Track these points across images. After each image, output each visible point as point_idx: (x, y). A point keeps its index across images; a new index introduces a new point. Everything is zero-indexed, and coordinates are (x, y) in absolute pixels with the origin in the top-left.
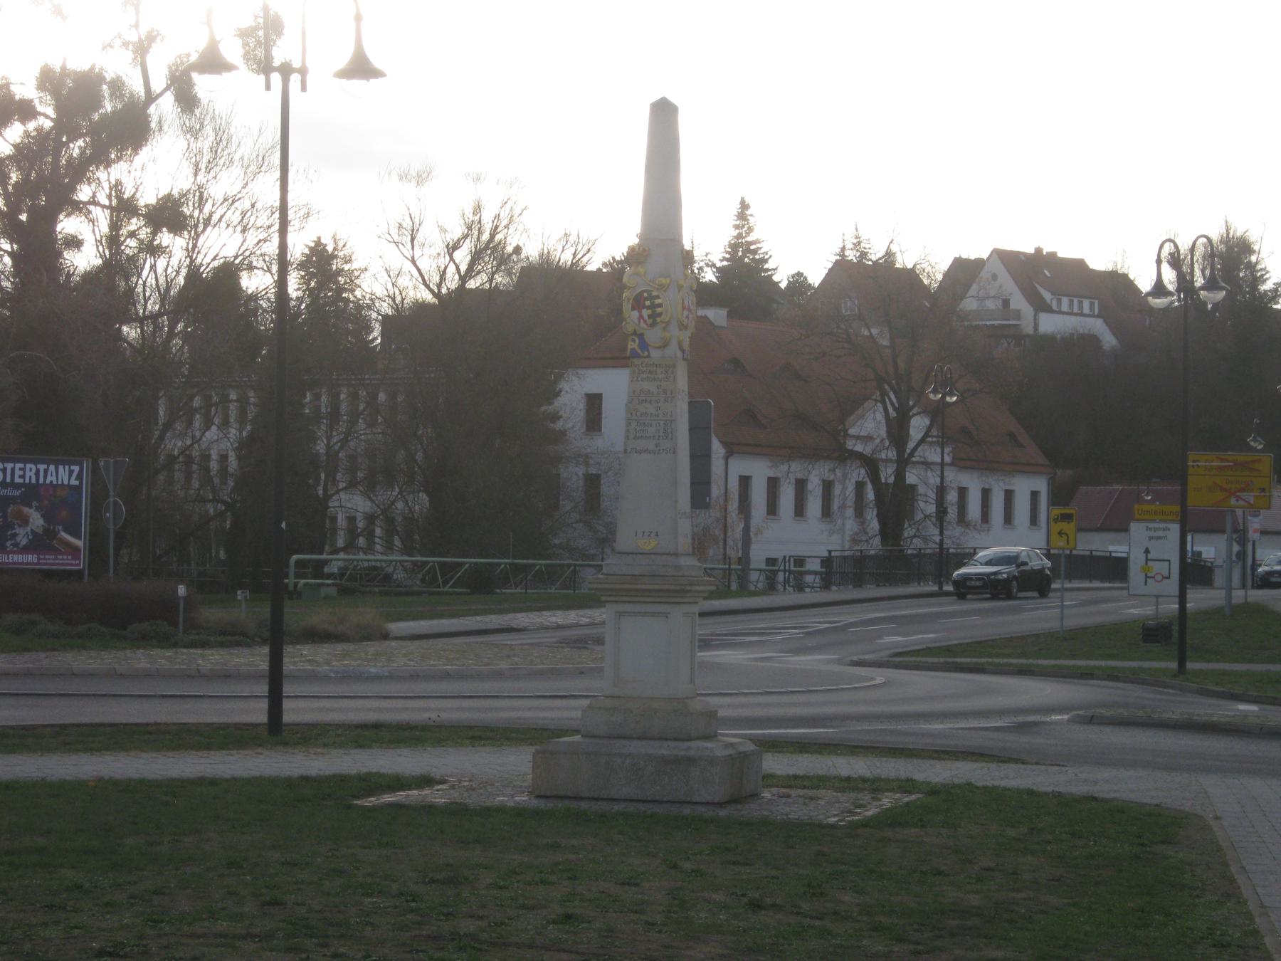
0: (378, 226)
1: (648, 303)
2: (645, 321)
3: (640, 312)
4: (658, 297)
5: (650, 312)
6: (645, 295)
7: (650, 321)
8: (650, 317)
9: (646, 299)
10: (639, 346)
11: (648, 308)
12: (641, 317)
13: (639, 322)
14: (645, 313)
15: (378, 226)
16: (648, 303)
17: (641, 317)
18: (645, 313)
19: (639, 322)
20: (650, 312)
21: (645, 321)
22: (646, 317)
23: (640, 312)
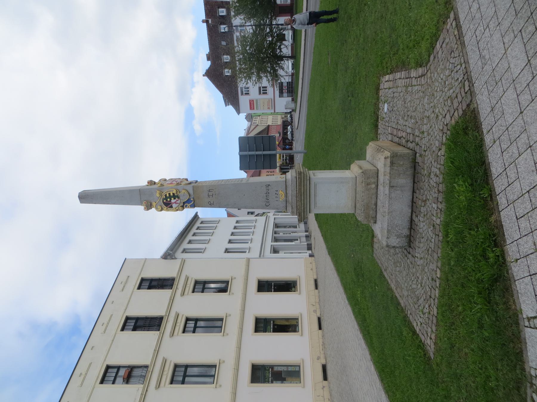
1: (169, 200)
3: (173, 203)
5: (172, 199)
6: (165, 201)
9: (167, 200)
10: (189, 204)
11: (171, 200)
12: (175, 203)
13: (177, 203)
16: (169, 200)
17: (175, 203)
18: (173, 201)
19: (177, 203)
20: (172, 199)
21: (177, 201)
22: (175, 200)
23: (173, 203)
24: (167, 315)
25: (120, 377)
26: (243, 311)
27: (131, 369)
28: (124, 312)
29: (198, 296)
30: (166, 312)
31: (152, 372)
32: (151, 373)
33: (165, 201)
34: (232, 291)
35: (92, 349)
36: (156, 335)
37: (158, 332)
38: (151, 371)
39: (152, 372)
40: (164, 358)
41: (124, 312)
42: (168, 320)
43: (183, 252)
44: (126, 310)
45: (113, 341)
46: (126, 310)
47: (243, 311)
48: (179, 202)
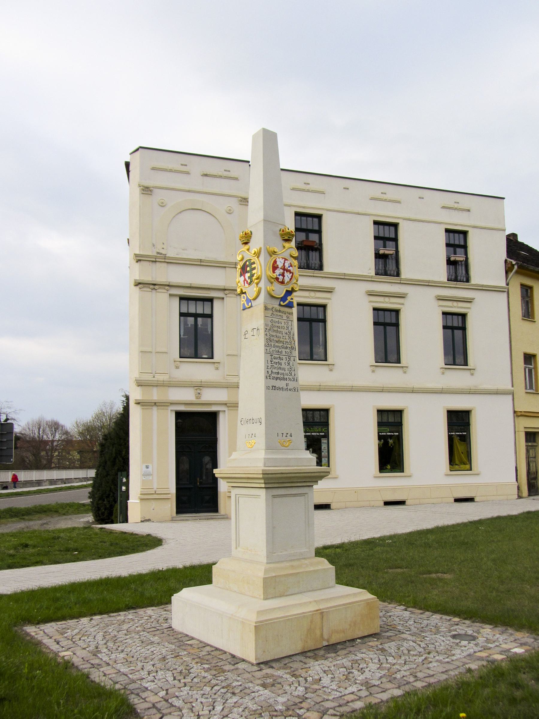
0: (163, 243)
2: (247, 282)
3: (244, 277)
4: (254, 263)
7: (249, 281)
8: (249, 278)
9: (248, 266)
12: (245, 280)
14: (248, 275)
15: (163, 243)
17: (245, 280)
18: (248, 275)
23: (244, 277)
24: (402, 282)
25: (307, 237)
26: (413, 391)
27: (318, 249)
28: (404, 219)
29: (438, 322)
30: (406, 279)
31: (314, 276)
32: (311, 276)
33: (248, 263)
34: (448, 372)
35: (345, 188)
36: (370, 271)
37: (373, 273)
38: (315, 275)
39: (314, 276)
40: (334, 289)
41: (404, 219)
42: (393, 284)
43: (522, 285)
44: (409, 220)
45: (358, 214)
46: (409, 220)
47: (413, 391)
48: (247, 285)
